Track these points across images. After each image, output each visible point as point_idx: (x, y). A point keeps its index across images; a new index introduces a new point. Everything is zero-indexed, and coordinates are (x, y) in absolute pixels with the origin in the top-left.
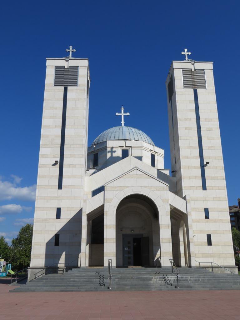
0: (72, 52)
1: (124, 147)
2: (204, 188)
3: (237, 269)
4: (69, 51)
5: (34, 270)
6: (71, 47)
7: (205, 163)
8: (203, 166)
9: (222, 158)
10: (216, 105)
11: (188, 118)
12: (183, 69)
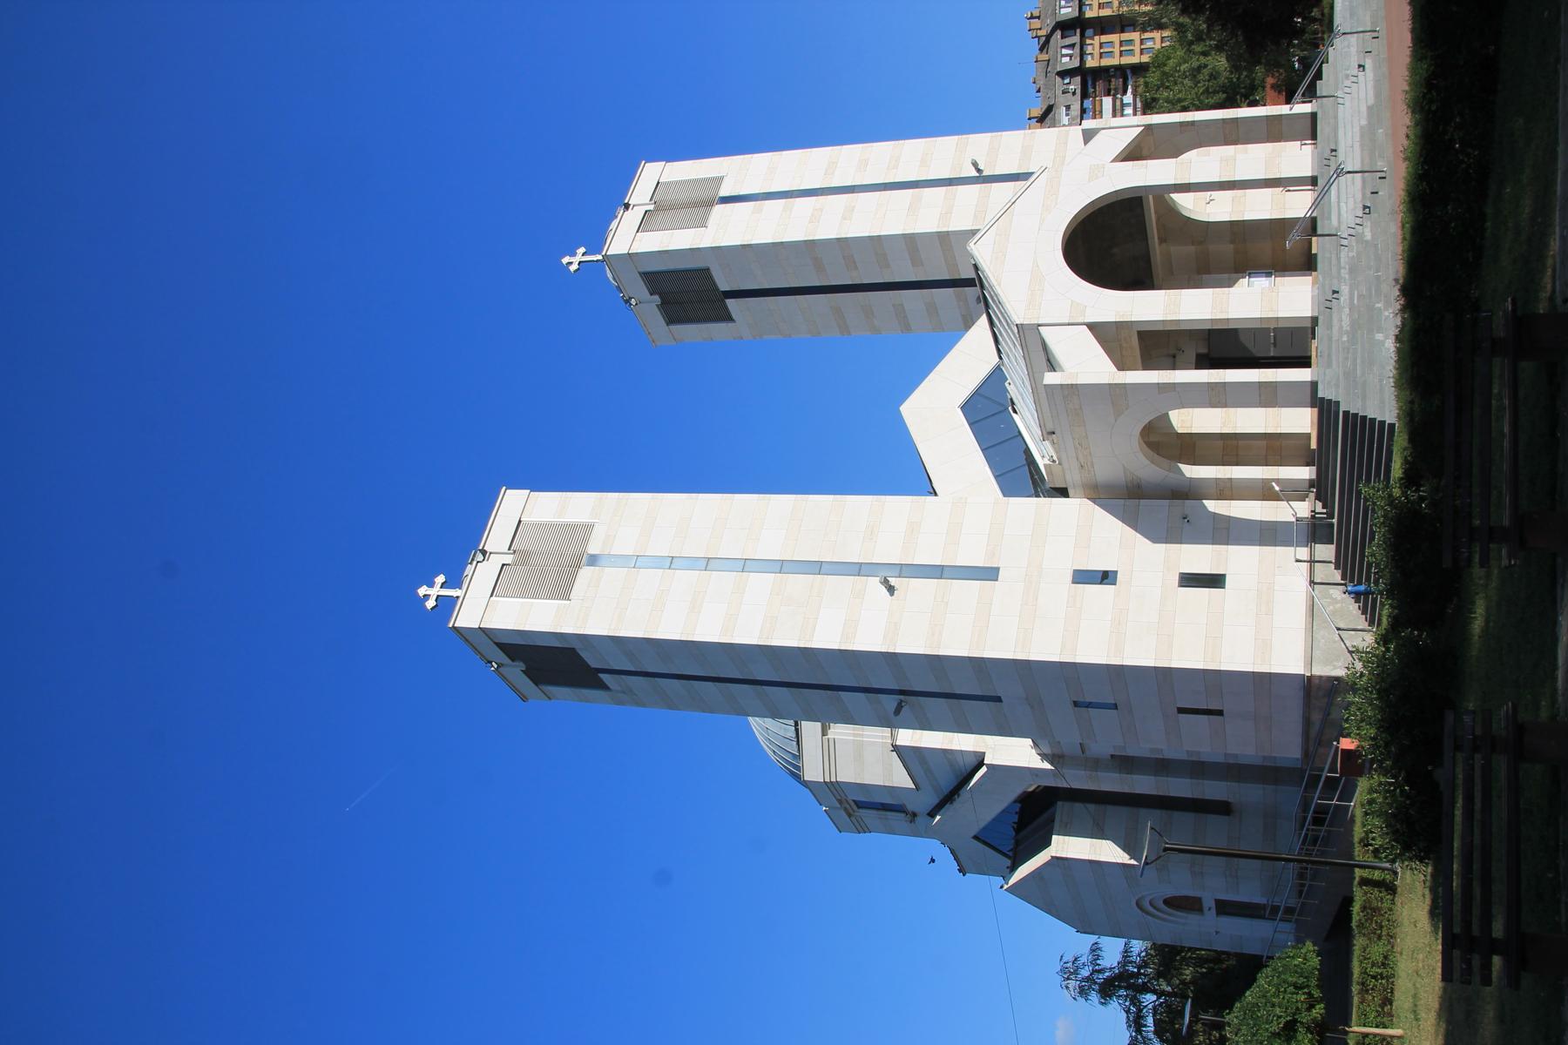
5: (1317, 653)
7: (975, 173)
8: (982, 179)
10: (784, 152)
11: (812, 215)
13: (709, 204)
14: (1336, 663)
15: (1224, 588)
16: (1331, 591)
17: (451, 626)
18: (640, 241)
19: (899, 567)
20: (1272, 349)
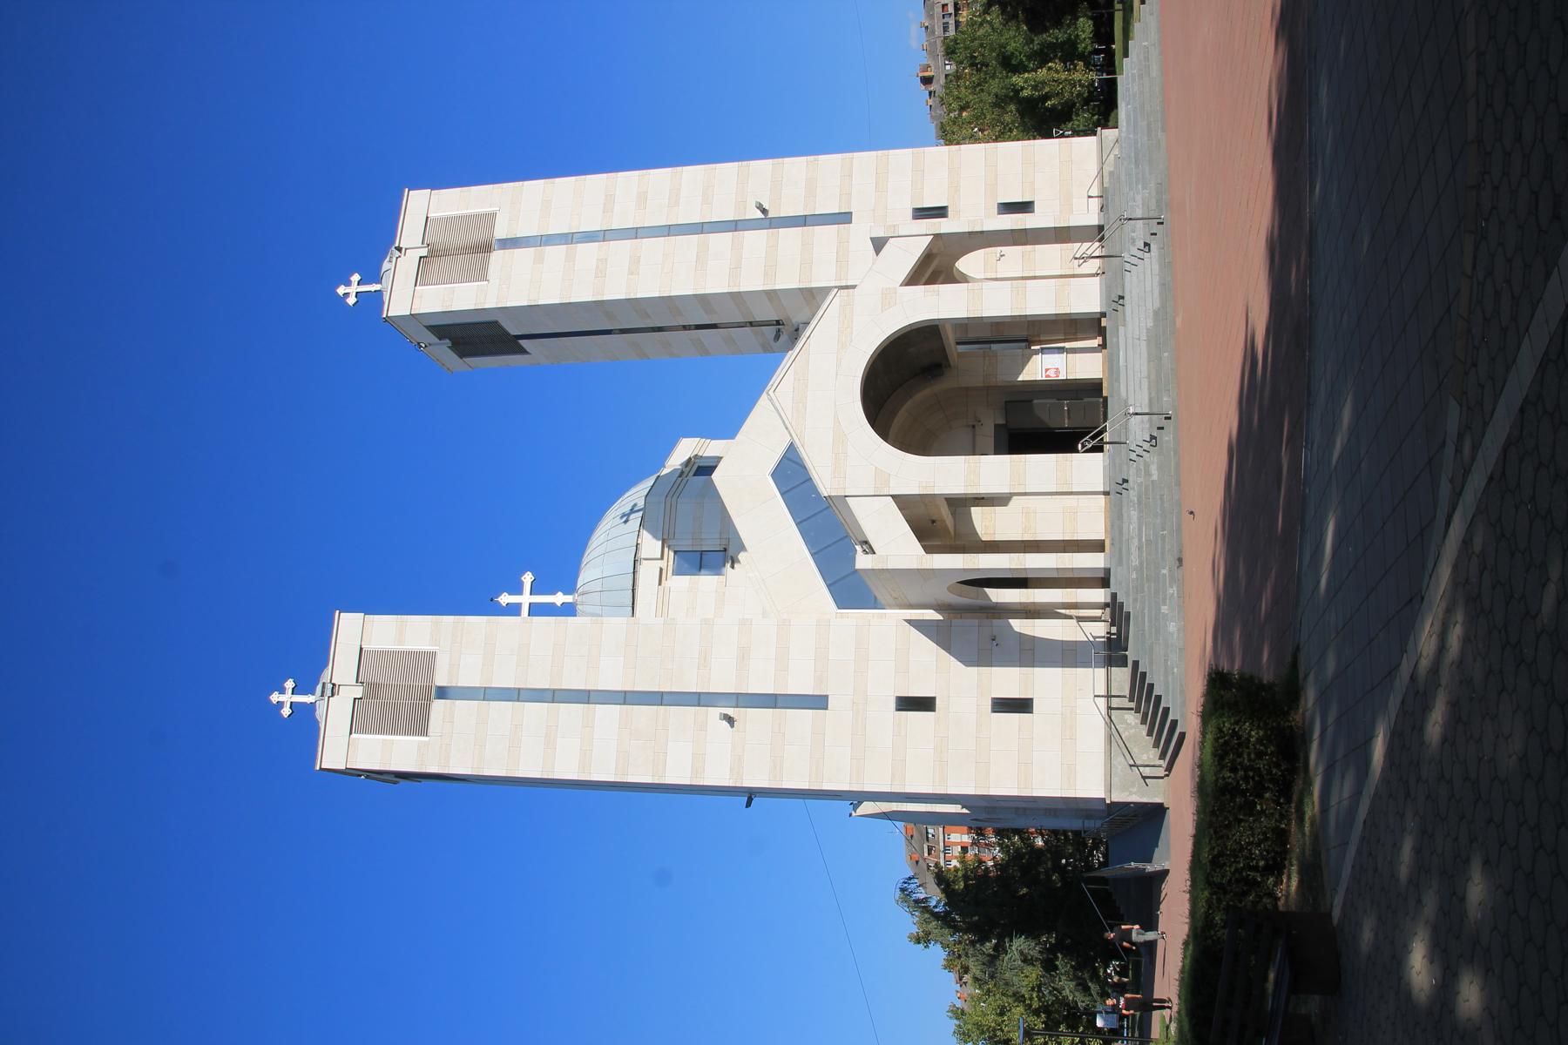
1: (663, 564)
3: (1106, 132)
5: (1115, 780)
6: (275, 697)
7: (759, 215)
8: (768, 221)
9: (745, 163)
10: (558, 180)
11: (597, 267)
12: (416, 285)
13: (486, 248)
14: (1131, 789)
15: (1032, 713)
16: (1126, 716)
17: (318, 768)
18: (421, 297)
19: (735, 696)
20: (1066, 421)
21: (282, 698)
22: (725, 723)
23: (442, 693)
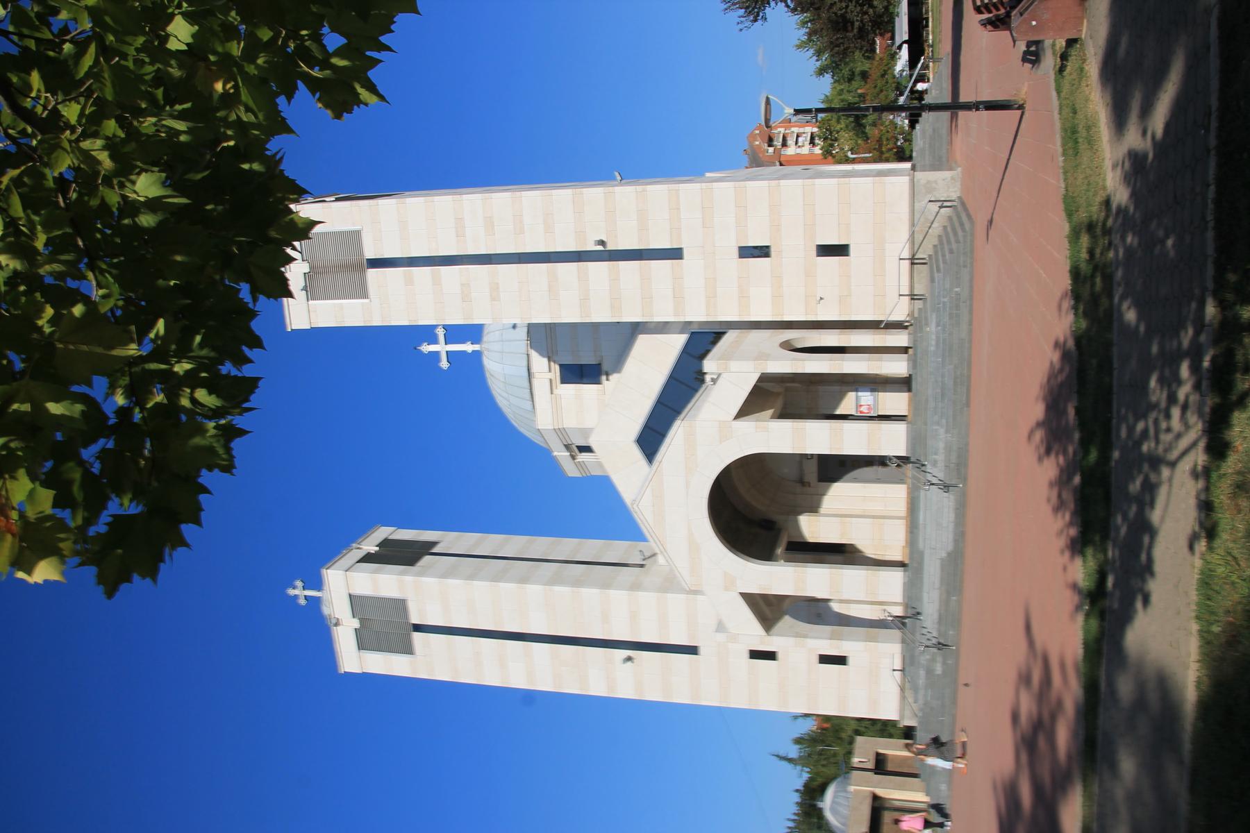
0: (304, 589)
2: (675, 254)
4: (305, 596)
6: (291, 592)
21: (296, 592)
22: (629, 663)
23: (418, 628)
